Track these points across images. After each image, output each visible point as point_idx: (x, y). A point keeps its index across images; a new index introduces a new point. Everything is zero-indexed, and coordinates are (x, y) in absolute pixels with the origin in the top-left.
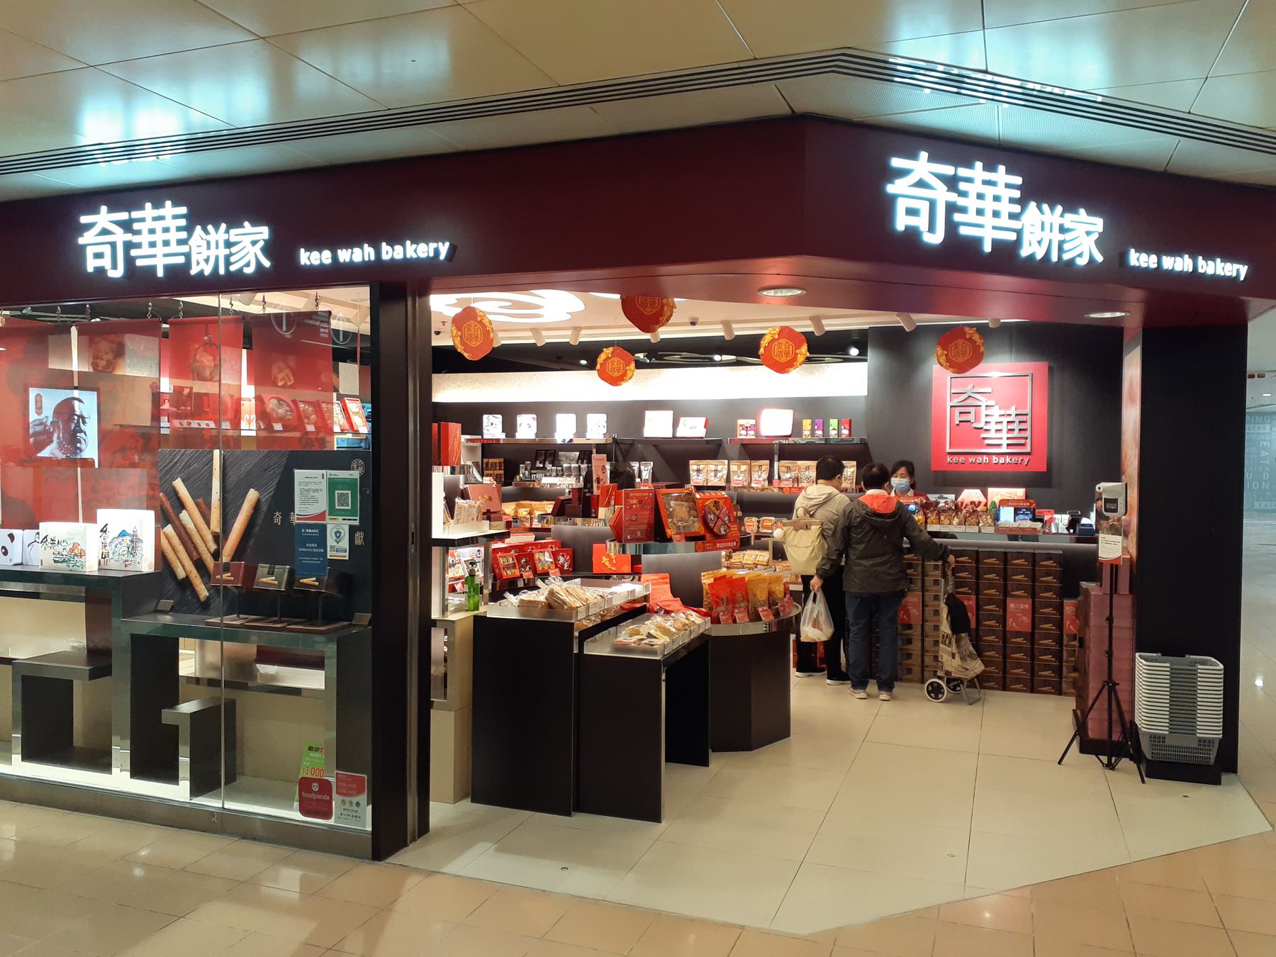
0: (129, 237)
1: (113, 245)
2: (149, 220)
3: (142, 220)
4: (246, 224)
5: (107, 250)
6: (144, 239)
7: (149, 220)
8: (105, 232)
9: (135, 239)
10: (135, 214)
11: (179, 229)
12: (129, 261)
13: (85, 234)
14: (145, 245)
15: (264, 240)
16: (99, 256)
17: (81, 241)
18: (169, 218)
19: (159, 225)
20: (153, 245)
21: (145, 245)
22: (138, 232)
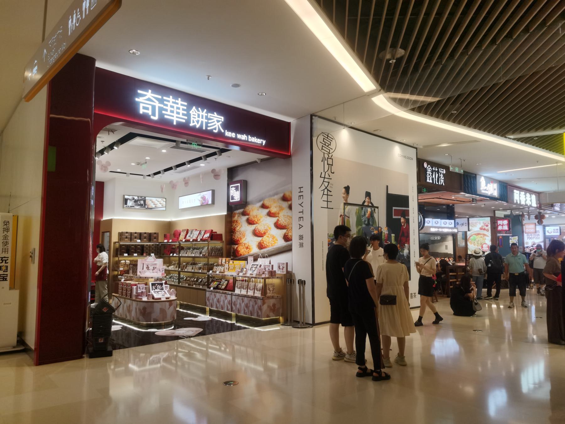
0: (162, 106)
1: (154, 107)
2: (171, 102)
3: (169, 101)
4: (215, 113)
5: (150, 107)
6: (169, 108)
7: (171, 102)
8: (149, 99)
9: (165, 107)
10: (165, 98)
11: (183, 110)
12: (161, 115)
13: (140, 98)
14: (169, 111)
15: (222, 121)
16: (148, 109)
17: (137, 99)
18: (179, 104)
19: (175, 106)
20: (172, 112)
21: (169, 111)
22: (167, 105)
